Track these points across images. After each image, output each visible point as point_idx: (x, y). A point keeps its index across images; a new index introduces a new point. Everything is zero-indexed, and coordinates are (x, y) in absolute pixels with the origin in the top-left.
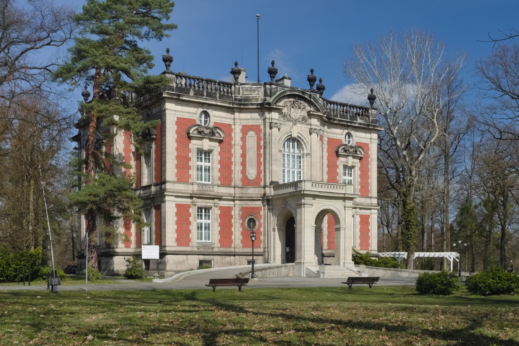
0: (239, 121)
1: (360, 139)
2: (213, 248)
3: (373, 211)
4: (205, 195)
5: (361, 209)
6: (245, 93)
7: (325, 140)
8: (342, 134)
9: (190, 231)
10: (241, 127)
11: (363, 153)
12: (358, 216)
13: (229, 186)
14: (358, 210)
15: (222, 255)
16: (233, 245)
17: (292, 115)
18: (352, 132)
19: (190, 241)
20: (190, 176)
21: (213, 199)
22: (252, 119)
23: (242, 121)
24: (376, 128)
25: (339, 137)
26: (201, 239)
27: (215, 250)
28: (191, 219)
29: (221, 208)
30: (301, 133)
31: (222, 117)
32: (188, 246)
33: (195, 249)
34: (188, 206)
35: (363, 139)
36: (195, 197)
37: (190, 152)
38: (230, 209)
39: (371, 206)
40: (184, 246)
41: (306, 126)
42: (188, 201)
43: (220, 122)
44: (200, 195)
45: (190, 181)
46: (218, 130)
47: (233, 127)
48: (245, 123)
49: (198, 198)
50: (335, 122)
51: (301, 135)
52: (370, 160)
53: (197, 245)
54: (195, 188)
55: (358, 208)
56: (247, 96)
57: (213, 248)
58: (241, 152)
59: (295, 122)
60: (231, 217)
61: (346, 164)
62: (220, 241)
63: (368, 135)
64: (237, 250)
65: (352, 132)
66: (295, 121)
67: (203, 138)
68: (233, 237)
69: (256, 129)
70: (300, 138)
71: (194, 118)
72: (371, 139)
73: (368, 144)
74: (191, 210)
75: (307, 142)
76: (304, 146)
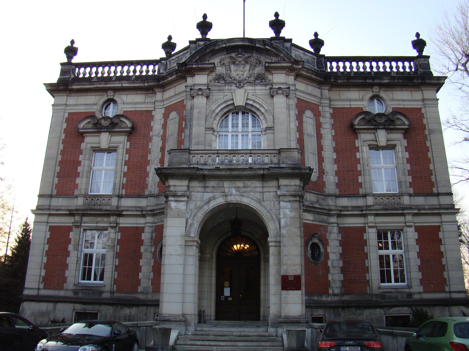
0: (162, 104)
1: (402, 103)
2: (101, 292)
4: (91, 210)
5: (414, 215)
6: (172, 66)
7: (327, 112)
8: (362, 100)
9: (66, 266)
10: (163, 111)
11: (407, 123)
12: (413, 229)
13: (140, 196)
14: (409, 218)
15: (117, 305)
16: (140, 289)
17: (234, 74)
18: (382, 94)
19: (66, 282)
20: (76, 186)
21: (108, 215)
22: (176, 95)
23: (165, 103)
24: (428, 81)
25: (355, 104)
26: (89, 279)
27: (106, 295)
28: (70, 247)
29: (123, 230)
30: (254, 98)
31: (136, 103)
32: (61, 288)
33: (70, 294)
34: (69, 229)
35: (405, 103)
36: (78, 214)
37: (82, 154)
38: (140, 230)
39: (440, 209)
40: (53, 289)
41: (264, 88)
42: (67, 221)
43: (134, 109)
44: (83, 210)
45: (75, 194)
46: (123, 119)
47: (153, 113)
48: (167, 104)
49: (83, 215)
50: (339, 81)
51: (254, 101)
52: (427, 132)
53: (75, 288)
54: (80, 202)
55: (409, 214)
56: (173, 69)
57: (101, 292)
58: (160, 144)
59: (240, 84)
60: (141, 242)
61: (375, 143)
62: (115, 281)
63: (417, 95)
64: (141, 297)
65: (383, 94)
66: (240, 82)
67: (100, 132)
68: (141, 274)
69: (179, 107)
70: (252, 105)
71: (94, 111)
72: (423, 100)
73: (420, 109)
74: (72, 235)
75: (266, 111)
76: (261, 117)
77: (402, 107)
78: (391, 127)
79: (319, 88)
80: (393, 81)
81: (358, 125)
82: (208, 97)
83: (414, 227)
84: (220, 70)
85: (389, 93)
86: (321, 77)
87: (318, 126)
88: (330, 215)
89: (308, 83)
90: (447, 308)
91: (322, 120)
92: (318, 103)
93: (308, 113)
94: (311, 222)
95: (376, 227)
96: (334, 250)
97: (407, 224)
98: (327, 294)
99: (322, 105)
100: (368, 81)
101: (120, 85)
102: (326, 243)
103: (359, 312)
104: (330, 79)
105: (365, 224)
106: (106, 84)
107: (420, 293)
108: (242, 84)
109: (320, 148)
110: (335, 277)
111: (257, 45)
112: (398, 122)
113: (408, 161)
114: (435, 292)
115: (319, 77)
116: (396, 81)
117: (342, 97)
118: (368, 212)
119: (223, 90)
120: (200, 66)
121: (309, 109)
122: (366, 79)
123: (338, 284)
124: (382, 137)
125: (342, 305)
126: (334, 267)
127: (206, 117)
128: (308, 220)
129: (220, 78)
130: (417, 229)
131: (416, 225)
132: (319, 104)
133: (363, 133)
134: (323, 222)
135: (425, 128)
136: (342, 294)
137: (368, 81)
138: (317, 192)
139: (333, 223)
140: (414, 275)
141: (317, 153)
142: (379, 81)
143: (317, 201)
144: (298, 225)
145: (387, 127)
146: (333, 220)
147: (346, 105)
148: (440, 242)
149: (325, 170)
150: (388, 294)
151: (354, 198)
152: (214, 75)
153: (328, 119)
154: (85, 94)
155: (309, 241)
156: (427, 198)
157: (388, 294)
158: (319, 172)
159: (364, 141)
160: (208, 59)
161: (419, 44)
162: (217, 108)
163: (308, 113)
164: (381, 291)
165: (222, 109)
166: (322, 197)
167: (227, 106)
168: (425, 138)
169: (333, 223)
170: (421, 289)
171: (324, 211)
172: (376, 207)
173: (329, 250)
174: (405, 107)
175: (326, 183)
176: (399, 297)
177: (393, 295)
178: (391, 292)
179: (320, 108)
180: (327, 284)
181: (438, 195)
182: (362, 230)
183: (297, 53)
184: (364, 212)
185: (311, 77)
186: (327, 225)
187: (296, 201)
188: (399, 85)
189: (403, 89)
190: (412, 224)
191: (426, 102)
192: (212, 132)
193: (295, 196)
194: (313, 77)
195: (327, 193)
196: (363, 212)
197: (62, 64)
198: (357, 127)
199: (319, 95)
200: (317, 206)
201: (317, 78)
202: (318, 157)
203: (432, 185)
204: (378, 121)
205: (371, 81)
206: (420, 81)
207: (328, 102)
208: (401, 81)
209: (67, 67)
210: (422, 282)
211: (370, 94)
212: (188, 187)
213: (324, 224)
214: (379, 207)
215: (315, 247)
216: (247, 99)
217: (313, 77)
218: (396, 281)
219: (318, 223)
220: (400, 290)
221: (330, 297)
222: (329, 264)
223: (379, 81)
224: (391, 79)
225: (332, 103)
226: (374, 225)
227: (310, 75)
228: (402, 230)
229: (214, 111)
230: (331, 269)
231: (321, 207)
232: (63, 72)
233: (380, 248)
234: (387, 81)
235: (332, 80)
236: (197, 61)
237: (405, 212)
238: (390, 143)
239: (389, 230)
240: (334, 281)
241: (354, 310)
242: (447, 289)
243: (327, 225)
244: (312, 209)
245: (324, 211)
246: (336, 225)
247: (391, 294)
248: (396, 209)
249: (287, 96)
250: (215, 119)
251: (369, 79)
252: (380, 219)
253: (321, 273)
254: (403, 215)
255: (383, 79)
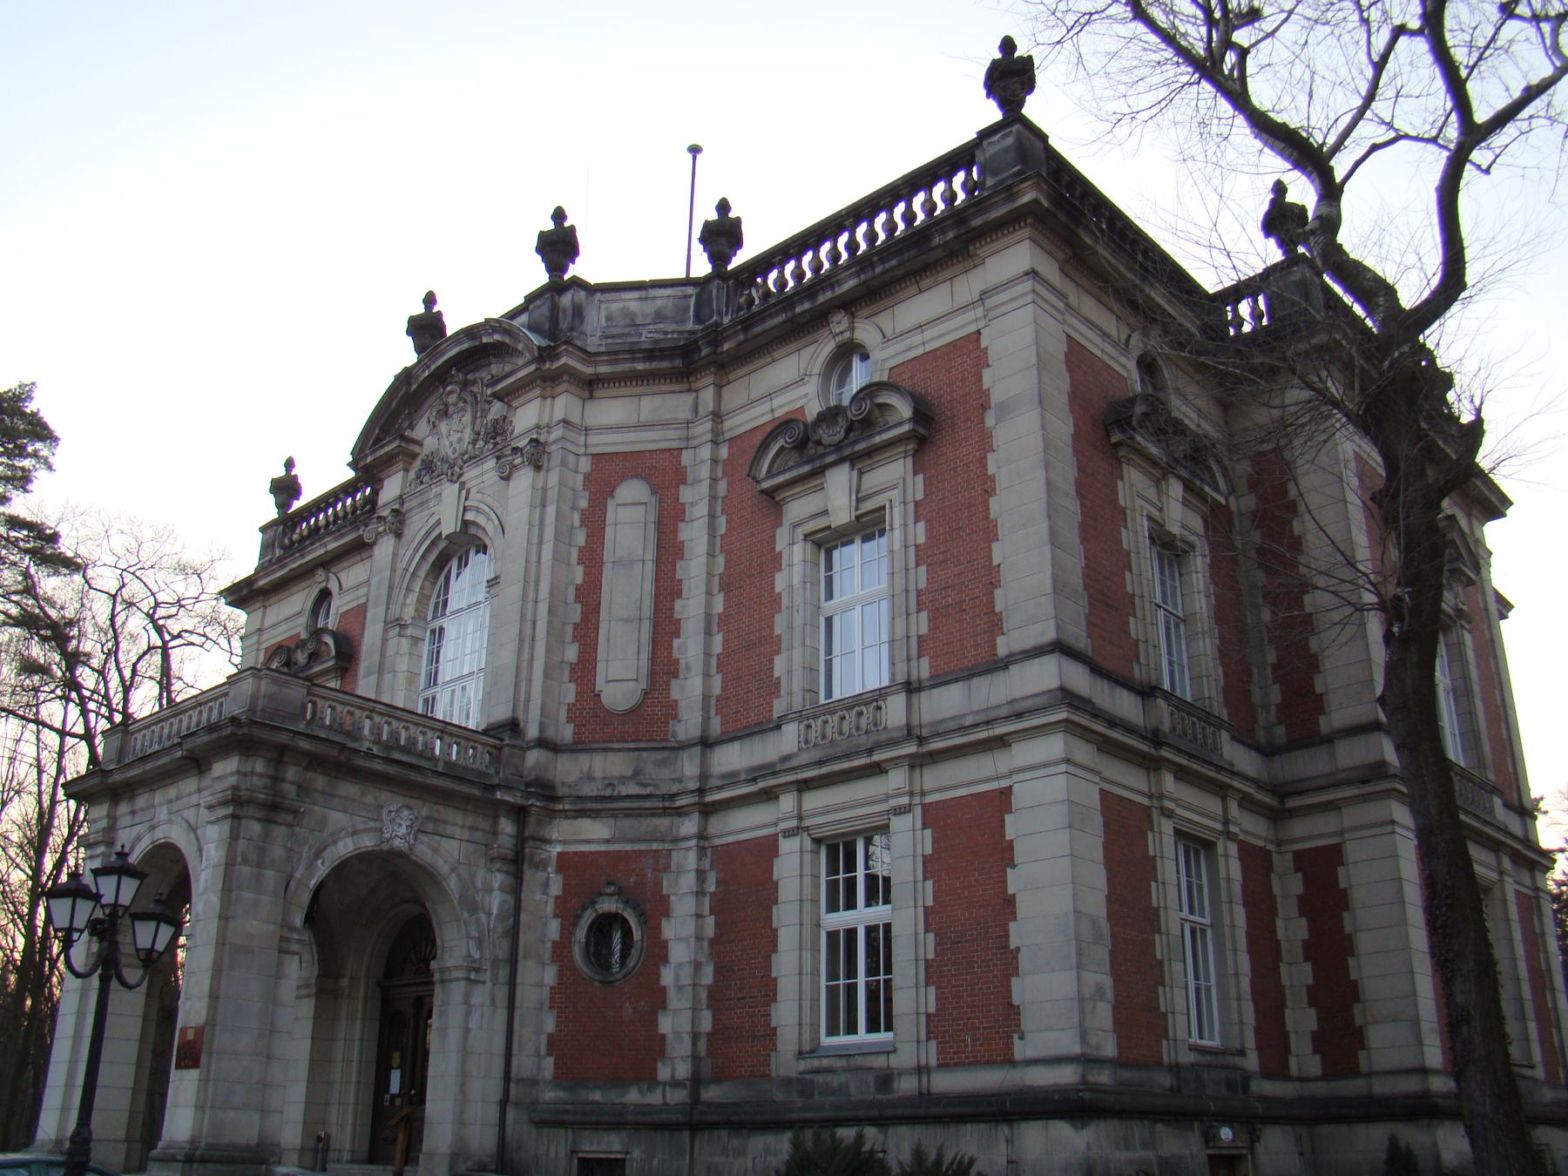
1: (917, 339)
3: (1026, 753)
5: (917, 763)
7: (699, 461)
8: (801, 381)
18: (865, 333)
25: (782, 405)
35: (928, 335)
50: (726, 347)
51: (478, 510)
52: (990, 420)
63: (968, 285)
65: (865, 333)
70: (474, 523)
77: (919, 351)
78: (858, 448)
79: (689, 390)
80: (870, 275)
81: (771, 474)
82: (399, 535)
83: (918, 810)
84: (430, 443)
85: (884, 320)
86: (671, 357)
87: (668, 521)
88: (680, 812)
89: (638, 390)
90: (1004, 1130)
91: (686, 495)
92: (675, 445)
93: (632, 491)
94: (602, 848)
95: (807, 829)
96: (684, 930)
97: (893, 803)
98: (653, 1082)
99: (695, 443)
100: (798, 310)
101: (322, 551)
102: (655, 908)
103: (736, 1142)
104: (699, 350)
105: (775, 824)
106: (303, 556)
107: (921, 1070)
108: (457, 469)
109: (667, 590)
110: (679, 1023)
111: (485, 340)
112: (892, 419)
113: (922, 555)
114: (975, 1063)
115: (662, 358)
116: (878, 270)
117: (755, 394)
118: (772, 782)
119: (427, 501)
120: (379, 453)
121: (636, 476)
122: (792, 307)
123: (685, 1048)
124: (837, 495)
125: (681, 1119)
126: (680, 988)
127: (391, 588)
128: (588, 842)
129: (428, 466)
130: (934, 816)
131: (929, 799)
132: (683, 444)
133: (794, 497)
134: (651, 841)
135: (984, 407)
136: (696, 1081)
137: (798, 310)
138: (633, 745)
139: (686, 839)
140: (911, 996)
141: (648, 611)
142: (829, 295)
143: (637, 773)
144: (220, 886)
145: (847, 452)
146: (689, 826)
147: (758, 416)
148: (1004, 854)
149: (682, 662)
150: (820, 1079)
151: (757, 738)
152: (418, 464)
153: (704, 488)
154: (287, 593)
155: (585, 909)
156: (975, 682)
157: (820, 1079)
158: (652, 674)
159: (795, 526)
160: (406, 424)
161: (1010, 77)
162: (412, 558)
163: (632, 491)
164: (803, 1065)
165: (423, 557)
166: (658, 755)
167: (434, 543)
168: (985, 443)
169: (686, 839)
170: (931, 1055)
171: (648, 804)
172: (804, 759)
173: (669, 930)
174: (929, 348)
175: (682, 705)
176: (853, 1089)
177: (835, 1080)
178: (830, 1070)
179: (686, 458)
180: (658, 1046)
181: (1004, 664)
182: (767, 849)
183: (615, 307)
184: (761, 785)
185: (633, 371)
186: (667, 846)
187: (226, 817)
188: (904, 277)
189: (925, 284)
190: (905, 800)
191: (989, 303)
192: (397, 630)
193: (224, 803)
194: (640, 367)
195: (681, 737)
196: (763, 787)
197: (263, 529)
198: (765, 485)
199: (685, 413)
200: (633, 789)
201: (654, 365)
202: (656, 624)
203: (995, 625)
204: (826, 439)
205: (807, 306)
206: (951, 235)
207: (708, 425)
208: (894, 262)
209: (271, 533)
210: (934, 1026)
211: (827, 347)
212: (113, 818)
213: (655, 846)
214: (815, 755)
215: (604, 926)
216: (465, 510)
217: (640, 367)
218: (873, 1027)
219: (628, 847)
220: (858, 1061)
221: (659, 1091)
222: (667, 977)
223: (829, 295)
224: (863, 270)
225: (727, 424)
226: (794, 823)
227: (626, 367)
228: (884, 829)
229: (406, 569)
230: (672, 994)
231: (649, 790)
232: (266, 548)
233: (833, 907)
234: (852, 283)
235: (704, 352)
236: (378, 440)
237: (876, 757)
238: (868, 506)
239: (858, 832)
240: (678, 1034)
241: (724, 1133)
242: (1020, 1050)
243: (667, 846)
244: (599, 806)
245: (648, 804)
246: (694, 842)
247: (828, 1077)
248: (848, 756)
249: (538, 468)
250: (408, 590)
251: (801, 302)
252: (815, 800)
253: (628, 1010)
254: (878, 769)
255: (839, 283)
